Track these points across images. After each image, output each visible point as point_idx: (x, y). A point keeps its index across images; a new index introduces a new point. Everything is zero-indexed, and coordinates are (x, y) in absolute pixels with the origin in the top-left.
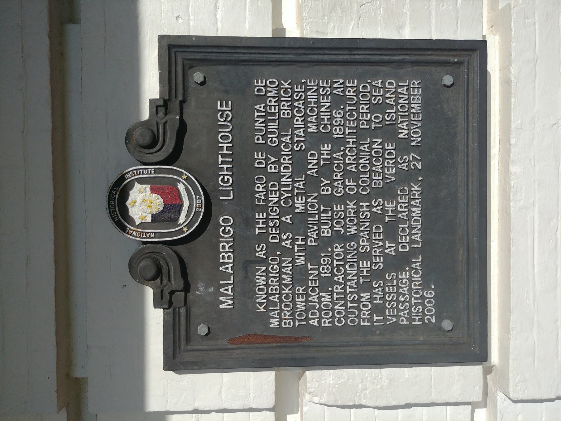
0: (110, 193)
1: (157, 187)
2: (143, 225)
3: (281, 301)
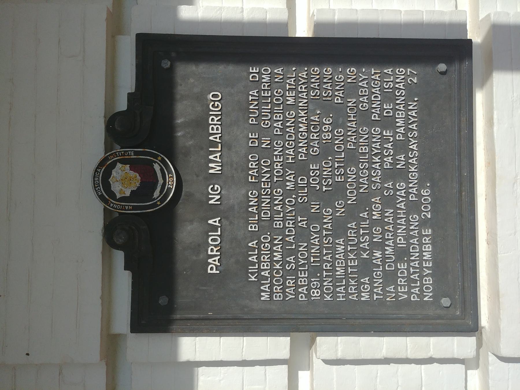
0: (96, 171)
1: (134, 165)
2: (124, 199)
3: (272, 277)
